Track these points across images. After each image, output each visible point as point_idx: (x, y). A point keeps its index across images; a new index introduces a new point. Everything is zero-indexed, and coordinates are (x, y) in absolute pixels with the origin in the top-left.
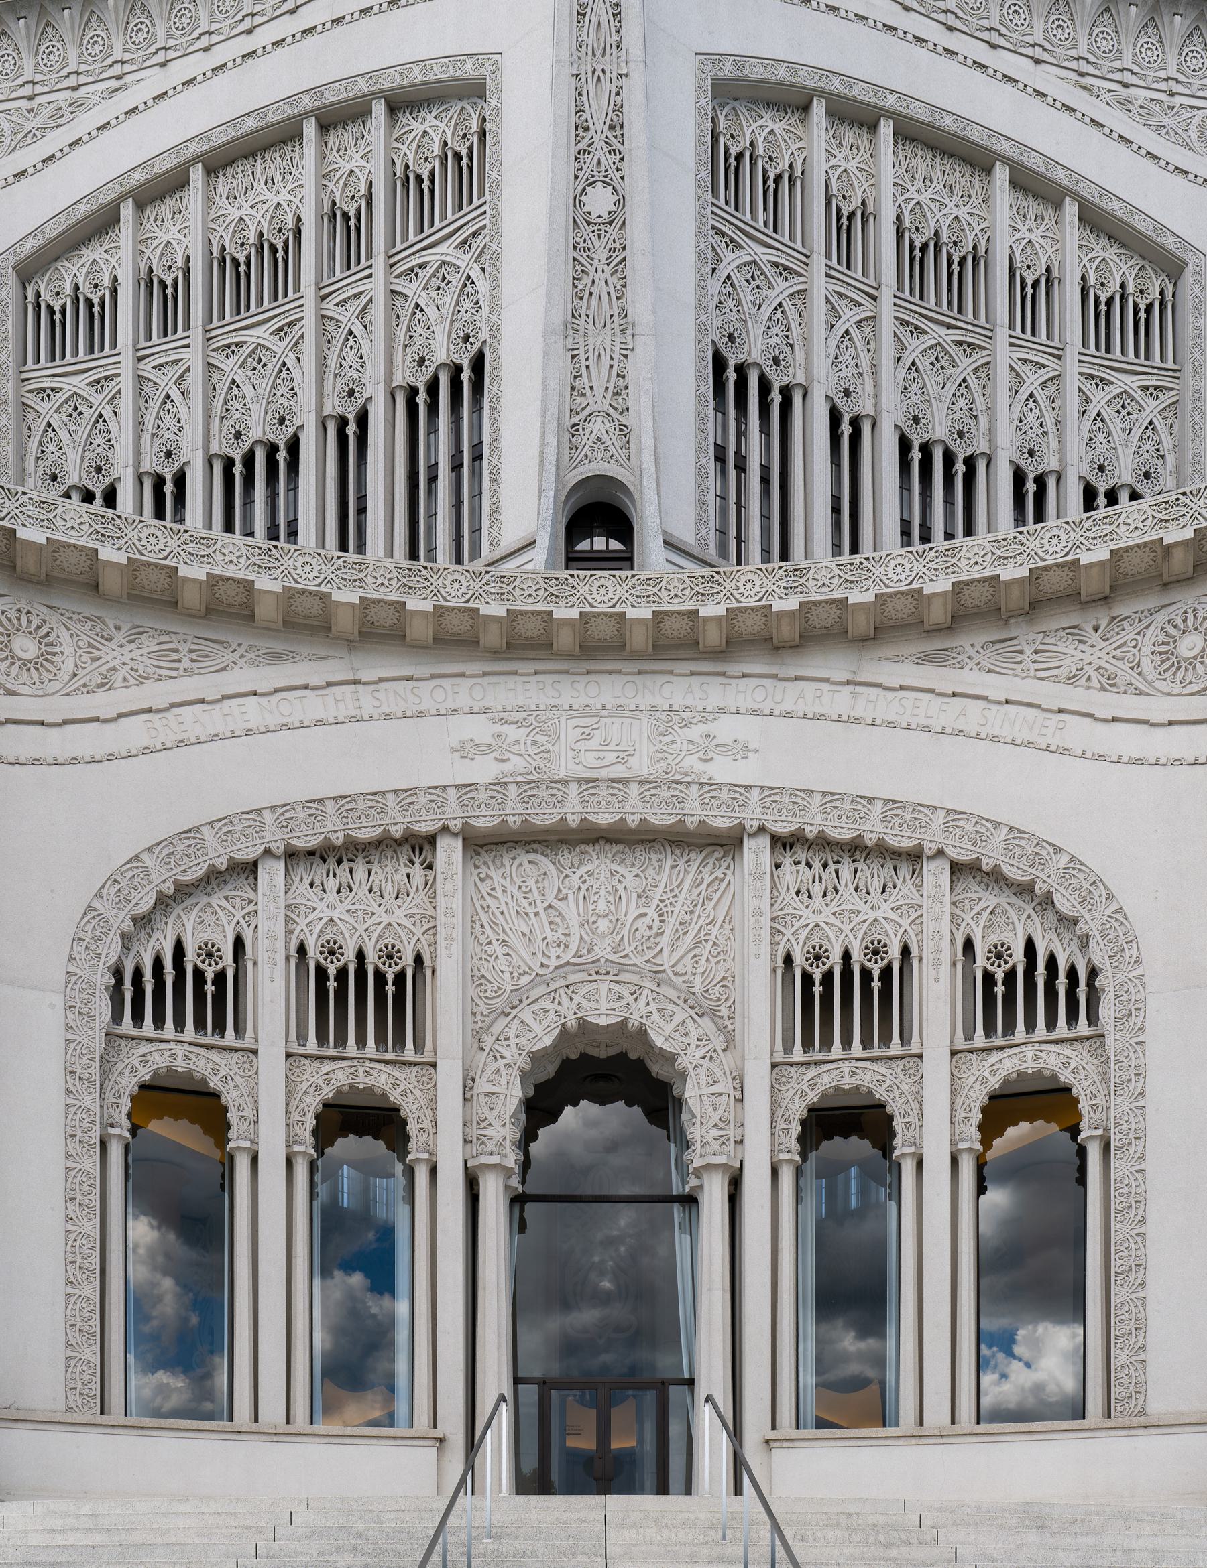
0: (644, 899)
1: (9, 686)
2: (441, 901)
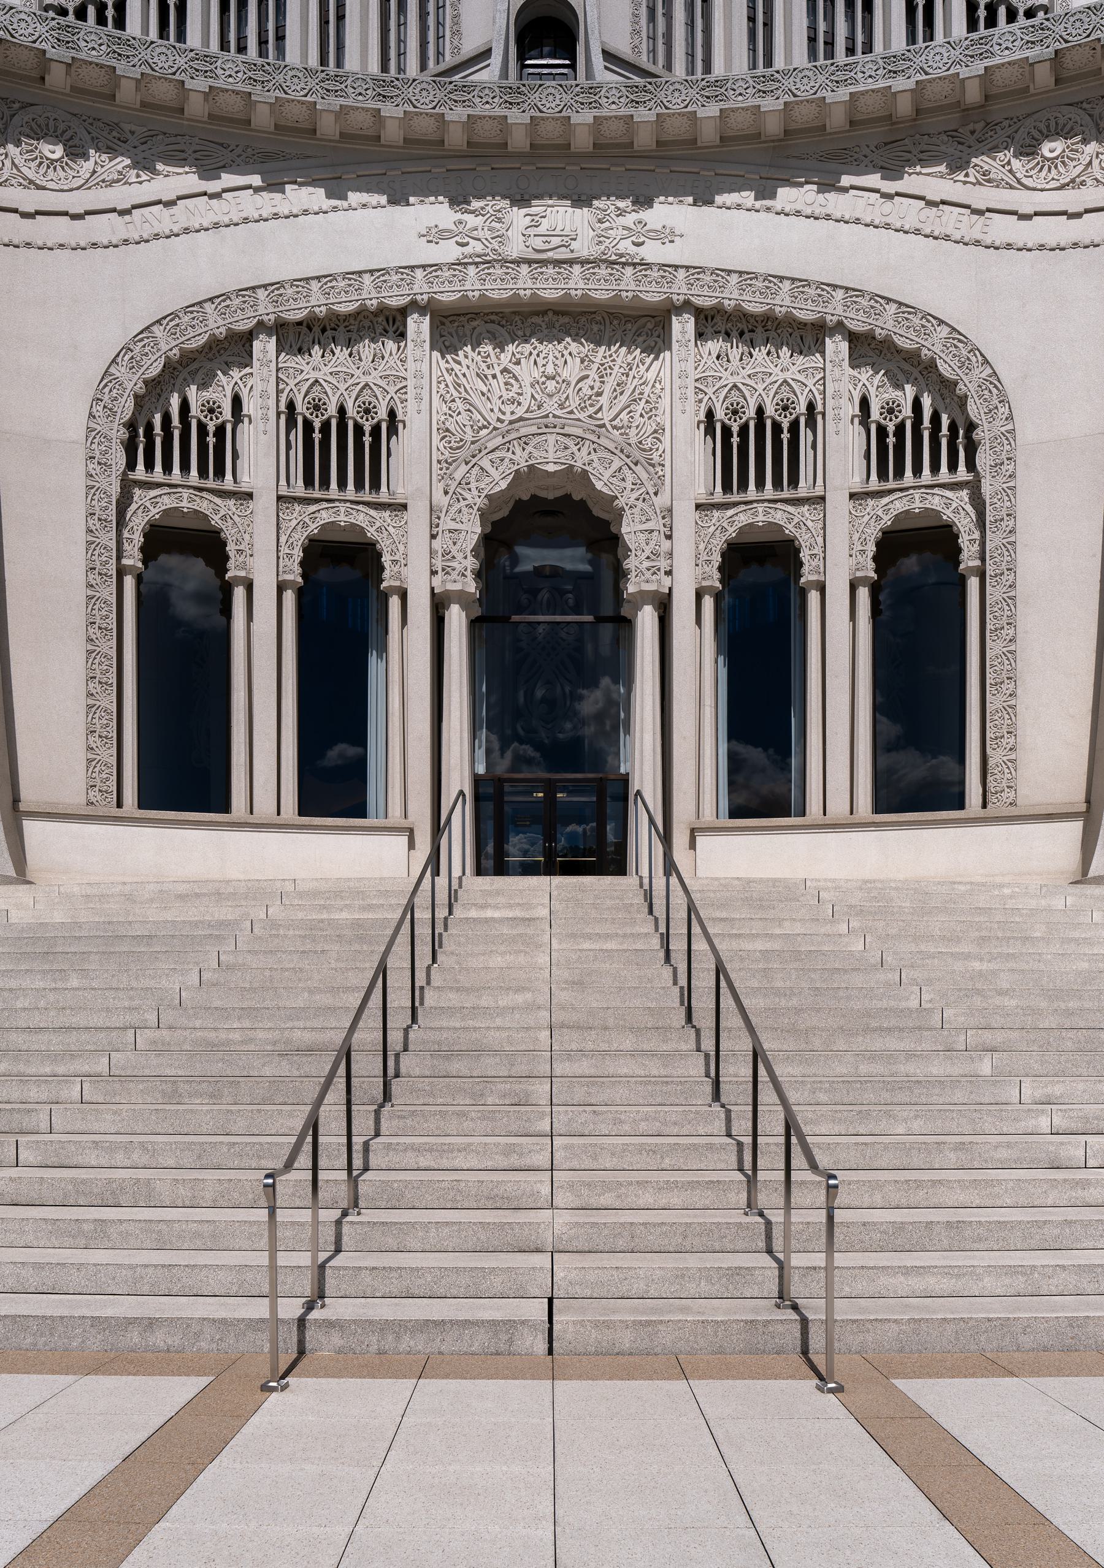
0: (586, 363)
1: (38, 182)
2: (410, 364)
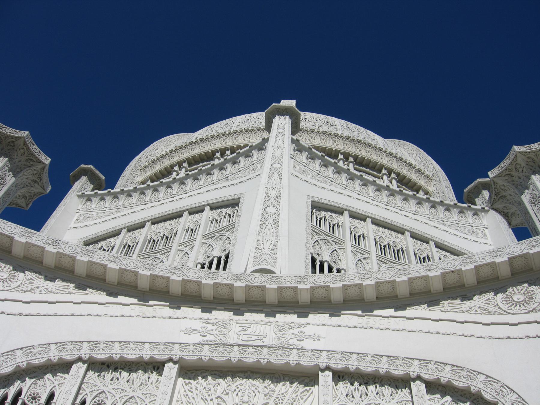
0: (268, 397)
